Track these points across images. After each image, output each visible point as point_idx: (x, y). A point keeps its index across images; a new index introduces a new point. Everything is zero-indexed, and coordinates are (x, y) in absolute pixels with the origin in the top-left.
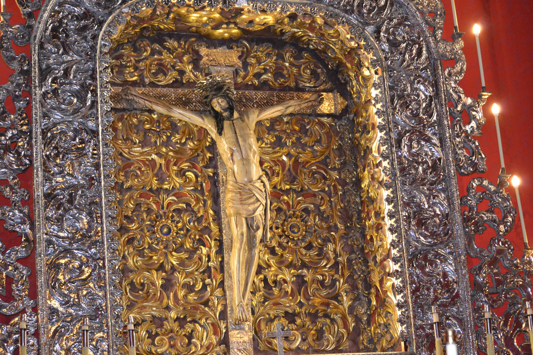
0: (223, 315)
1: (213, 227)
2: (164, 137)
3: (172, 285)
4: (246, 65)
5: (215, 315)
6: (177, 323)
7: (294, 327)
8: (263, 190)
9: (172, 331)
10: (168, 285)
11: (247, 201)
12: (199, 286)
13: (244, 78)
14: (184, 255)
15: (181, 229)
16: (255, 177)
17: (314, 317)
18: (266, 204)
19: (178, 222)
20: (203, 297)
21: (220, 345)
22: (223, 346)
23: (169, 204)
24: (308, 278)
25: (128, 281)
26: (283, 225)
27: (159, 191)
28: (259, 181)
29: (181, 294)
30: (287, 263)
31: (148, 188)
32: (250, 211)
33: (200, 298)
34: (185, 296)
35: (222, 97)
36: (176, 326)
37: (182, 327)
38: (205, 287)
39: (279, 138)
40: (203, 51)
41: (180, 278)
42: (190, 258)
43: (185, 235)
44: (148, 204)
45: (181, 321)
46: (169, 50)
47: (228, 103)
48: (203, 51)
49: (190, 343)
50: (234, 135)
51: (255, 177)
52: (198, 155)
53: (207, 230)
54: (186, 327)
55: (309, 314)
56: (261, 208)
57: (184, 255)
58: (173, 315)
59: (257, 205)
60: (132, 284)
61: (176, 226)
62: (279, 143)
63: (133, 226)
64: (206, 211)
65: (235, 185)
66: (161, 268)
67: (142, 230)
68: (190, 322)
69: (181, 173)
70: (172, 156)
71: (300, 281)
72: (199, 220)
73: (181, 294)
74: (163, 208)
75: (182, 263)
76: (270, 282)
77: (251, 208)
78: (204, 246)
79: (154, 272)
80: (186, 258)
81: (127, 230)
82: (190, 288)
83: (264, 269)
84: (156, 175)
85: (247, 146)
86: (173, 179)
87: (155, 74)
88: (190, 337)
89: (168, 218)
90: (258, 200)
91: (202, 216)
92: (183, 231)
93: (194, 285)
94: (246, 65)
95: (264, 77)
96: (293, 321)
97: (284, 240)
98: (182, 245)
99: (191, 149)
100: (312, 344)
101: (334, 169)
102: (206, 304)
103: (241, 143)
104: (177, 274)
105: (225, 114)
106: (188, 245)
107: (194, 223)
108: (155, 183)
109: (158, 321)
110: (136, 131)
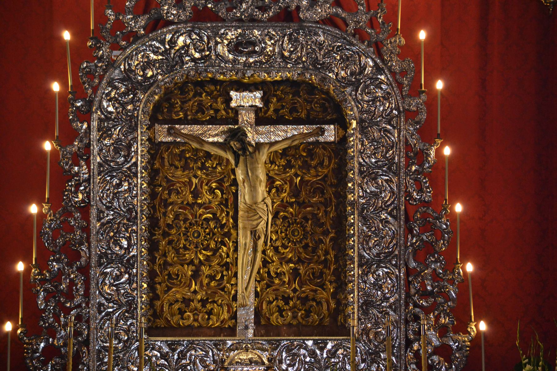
0: (235, 298)
2: (199, 163)
3: (200, 276)
5: (229, 298)
6: (200, 303)
7: (288, 308)
8: (266, 209)
9: (196, 309)
10: (196, 275)
11: (252, 218)
12: (219, 277)
13: (266, 112)
15: (209, 234)
16: (260, 199)
18: (268, 219)
19: (206, 229)
20: (221, 284)
21: (231, 320)
22: (233, 321)
23: (201, 215)
25: (166, 272)
26: (286, 230)
27: (192, 206)
28: (263, 203)
29: (206, 281)
30: (286, 259)
31: (185, 203)
32: (254, 225)
33: (219, 285)
34: (208, 284)
35: (236, 141)
36: (199, 305)
37: (204, 306)
38: (223, 276)
39: (289, 162)
40: (233, 94)
41: (205, 270)
42: (214, 255)
43: (211, 238)
44: (185, 214)
45: (204, 302)
46: (206, 92)
47: (241, 145)
48: (233, 94)
49: (209, 319)
50: (246, 168)
51: (260, 199)
52: (225, 177)
53: (228, 235)
54: (208, 306)
55: (299, 298)
56: (263, 222)
58: (199, 297)
59: (259, 221)
60: (169, 275)
61: (205, 232)
63: (173, 231)
64: (228, 220)
65: (244, 205)
66: (191, 262)
67: (180, 234)
68: (211, 302)
69: (212, 191)
70: (205, 179)
73: (206, 281)
74: (196, 218)
76: (272, 274)
77: (255, 223)
78: (225, 246)
79: (186, 266)
80: (211, 255)
81: (169, 235)
82: (212, 278)
83: (269, 263)
84: (191, 192)
85: (254, 177)
86: (204, 195)
87: (197, 112)
88: (210, 313)
89: (199, 226)
90: (261, 217)
91: (225, 224)
92: (210, 235)
93: (215, 276)
95: (281, 111)
96: (287, 303)
98: (208, 245)
99: (219, 173)
100: (301, 320)
101: (331, 185)
103: (250, 174)
104: (203, 268)
105: (240, 152)
106: (213, 245)
107: (218, 230)
108: (190, 199)
109: (187, 301)
110: (179, 159)
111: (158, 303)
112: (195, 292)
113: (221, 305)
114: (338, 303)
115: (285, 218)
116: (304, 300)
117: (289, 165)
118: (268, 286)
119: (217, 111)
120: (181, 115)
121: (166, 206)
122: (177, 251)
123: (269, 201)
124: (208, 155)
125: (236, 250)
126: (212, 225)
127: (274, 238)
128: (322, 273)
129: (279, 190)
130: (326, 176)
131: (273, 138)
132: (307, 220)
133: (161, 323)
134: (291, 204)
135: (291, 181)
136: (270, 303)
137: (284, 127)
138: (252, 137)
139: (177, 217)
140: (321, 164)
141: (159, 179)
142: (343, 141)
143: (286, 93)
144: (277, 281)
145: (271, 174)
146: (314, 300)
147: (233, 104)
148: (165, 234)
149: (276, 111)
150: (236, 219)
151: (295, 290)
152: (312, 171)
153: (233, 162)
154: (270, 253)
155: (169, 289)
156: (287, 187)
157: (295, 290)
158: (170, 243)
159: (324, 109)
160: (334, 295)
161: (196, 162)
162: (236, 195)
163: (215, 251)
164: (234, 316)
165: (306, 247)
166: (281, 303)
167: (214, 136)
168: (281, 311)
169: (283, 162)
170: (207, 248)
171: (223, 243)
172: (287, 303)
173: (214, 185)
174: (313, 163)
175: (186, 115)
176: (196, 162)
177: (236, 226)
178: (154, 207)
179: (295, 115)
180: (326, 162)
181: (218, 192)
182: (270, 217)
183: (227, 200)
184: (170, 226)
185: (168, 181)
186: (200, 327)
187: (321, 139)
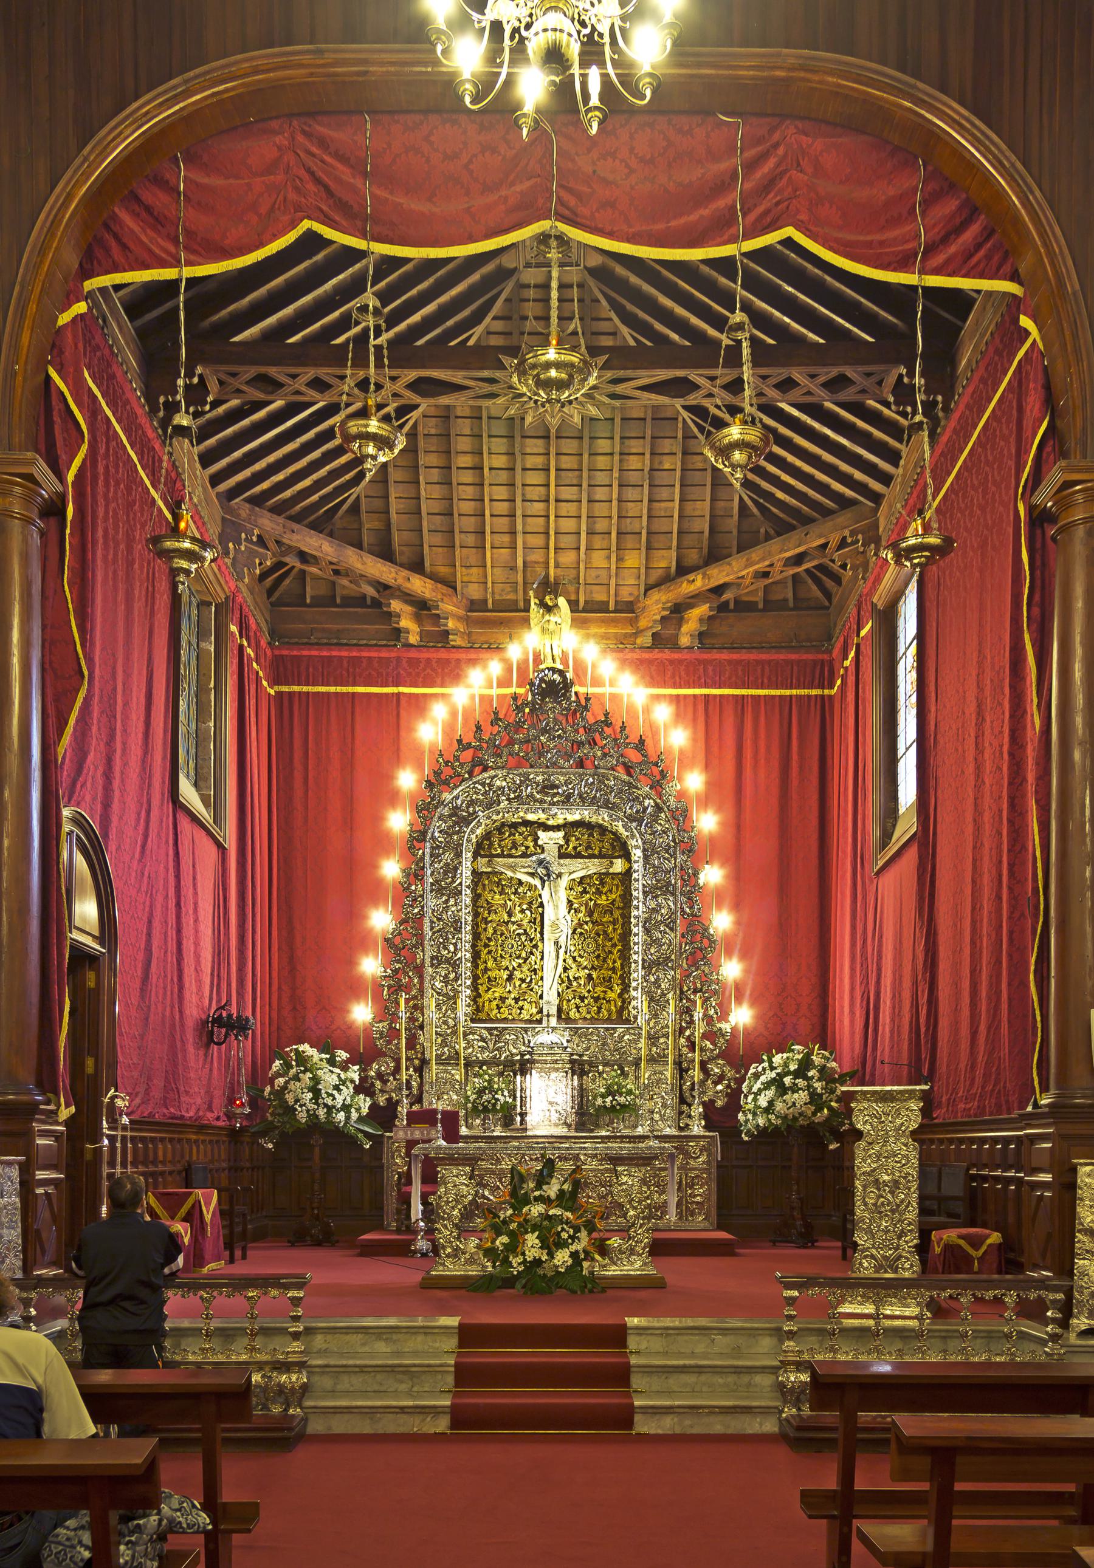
0: (541, 997)
1: (539, 944)
4: (567, 842)
10: (510, 978)
12: (528, 980)
14: (521, 961)
16: (561, 916)
17: (596, 999)
24: (594, 976)
27: (507, 923)
37: (516, 1003)
38: (531, 979)
39: (585, 888)
40: (540, 833)
45: (516, 1000)
48: (540, 833)
53: (536, 946)
57: (521, 961)
58: (513, 996)
60: (489, 978)
62: (585, 892)
63: (492, 943)
66: (507, 968)
69: (522, 911)
71: (590, 977)
72: (531, 940)
75: (520, 966)
82: (523, 981)
88: (521, 1008)
94: (567, 842)
96: (583, 1001)
97: (582, 952)
101: (618, 908)
102: (531, 990)
106: (524, 955)
108: (506, 918)
109: (503, 999)
111: (480, 1000)
112: (510, 992)
113: (530, 1002)
114: (624, 1002)
115: (581, 934)
116: (596, 999)
117: (585, 892)
118: (568, 988)
119: (527, 848)
120: (499, 851)
121: (487, 923)
122: (495, 960)
123: (569, 918)
124: (520, 883)
125: (542, 959)
126: (523, 938)
127: (573, 949)
128: (611, 978)
129: (577, 911)
130: (614, 900)
131: (573, 869)
132: (599, 935)
133: (482, 1016)
134: (586, 923)
135: (586, 905)
136: (569, 1001)
137: (581, 861)
138: (555, 868)
139: (495, 932)
140: (610, 891)
141: (481, 902)
142: (628, 873)
143: (583, 835)
144: (575, 984)
145: (571, 898)
146: (604, 999)
147: (540, 842)
148: (486, 946)
149: (575, 848)
150: (542, 933)
151: (589, 991)
152: (604, 897)
153: (539, 887)
154: (570, 961)
155: (489, 989)
156: (583, 908)
157: (589, 991)
158: (489, 952)
159: (614, 848)
160: (620, 995)
161: (510, 887)
162: (542, 915)
163: (526, 960)
164: (541, 1011)
165: (598, 957)
166: (578, 1001)
167: (525, 867)
168: (578, 1007)
169: (580, 889)
170: (519, 957)
171: (532, 953)
172: (583, 1001)
173: (525, 907)
174: (605, 890)
175: (503, 851)
176: (510, 887)
177: (542, 940)
178: (477, 924)
179: (590, 851)
180: (614, 889)
181: (528, 912)
182: (570, 932)
183: (535, 919)
184: (489, 939)
185: (488, 903)
186: (514, 1019)
187: (611, 871)
